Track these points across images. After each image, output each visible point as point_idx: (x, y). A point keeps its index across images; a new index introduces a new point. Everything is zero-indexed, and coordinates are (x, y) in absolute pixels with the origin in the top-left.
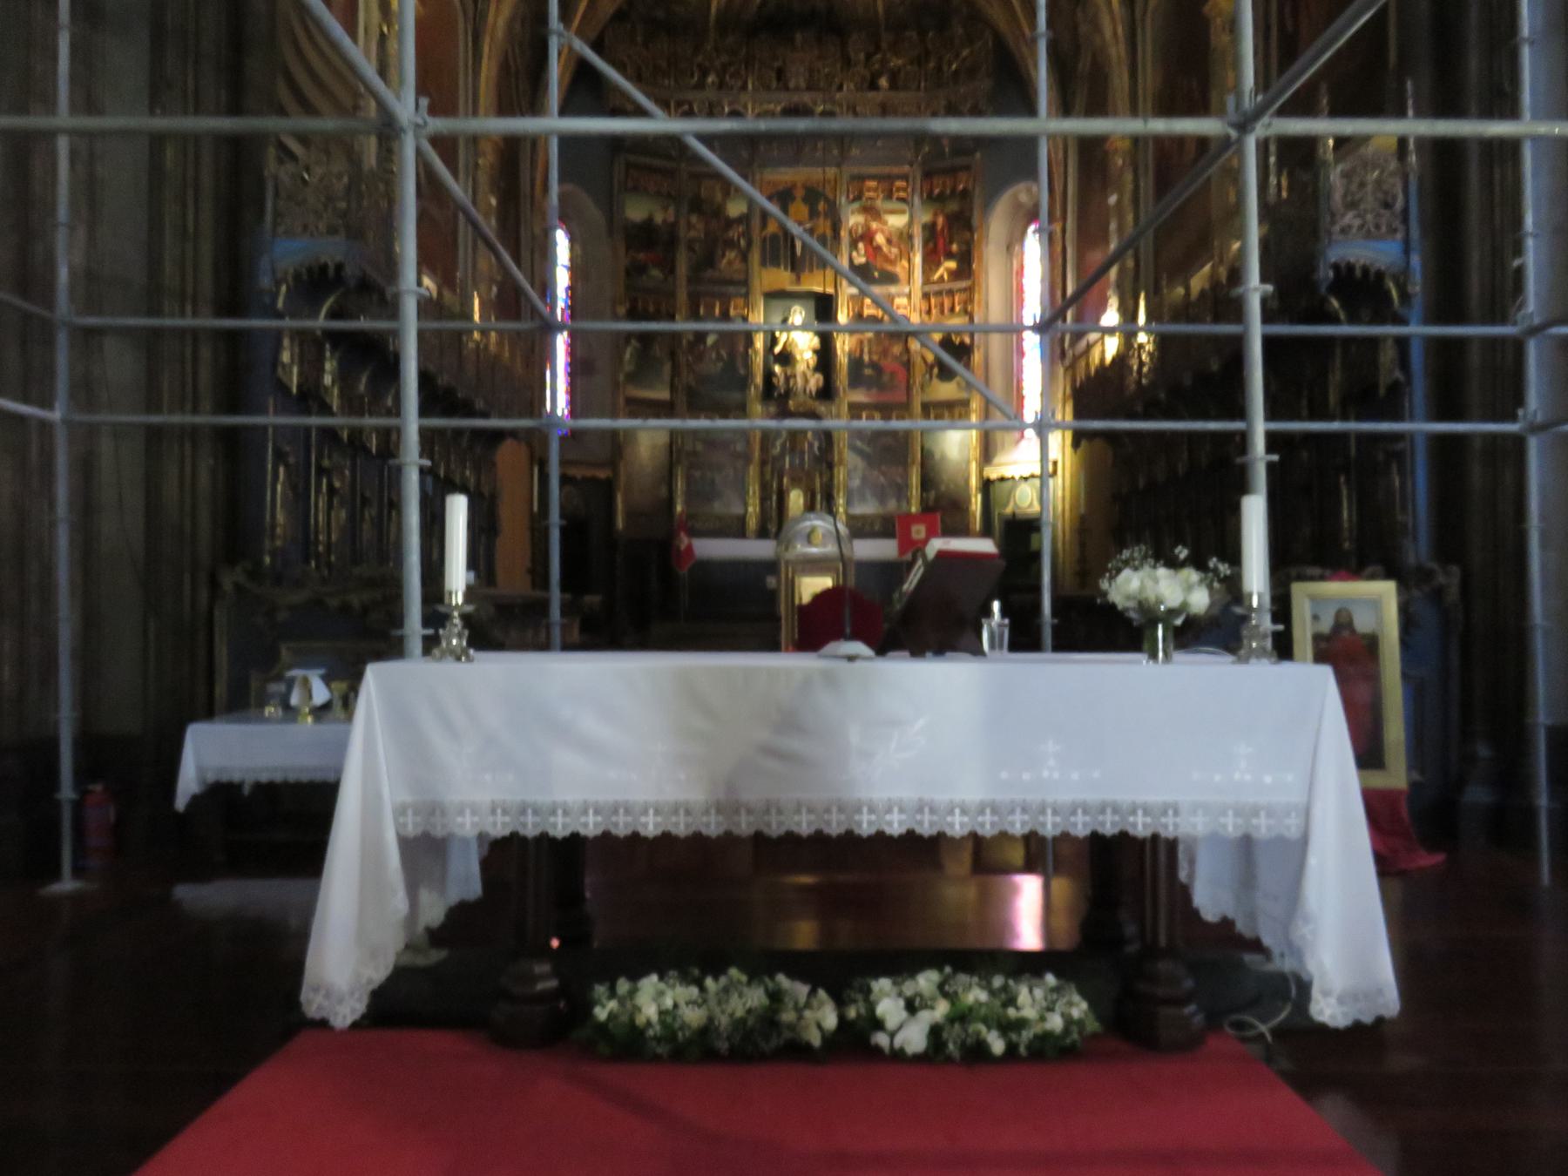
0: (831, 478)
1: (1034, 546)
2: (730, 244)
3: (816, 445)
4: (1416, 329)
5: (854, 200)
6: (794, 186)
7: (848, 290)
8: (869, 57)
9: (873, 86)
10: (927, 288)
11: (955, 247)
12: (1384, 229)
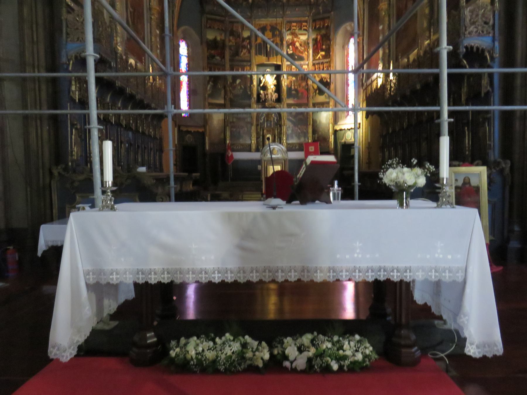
1: (352, 154)
2: (244, 47)
3: (276, 118)
4: (496, 70)
5: (288, 30)
6: (267, 25)
7: (286, 63)
10: (314, 62)
11: (324, 47)
12: (485, 32)
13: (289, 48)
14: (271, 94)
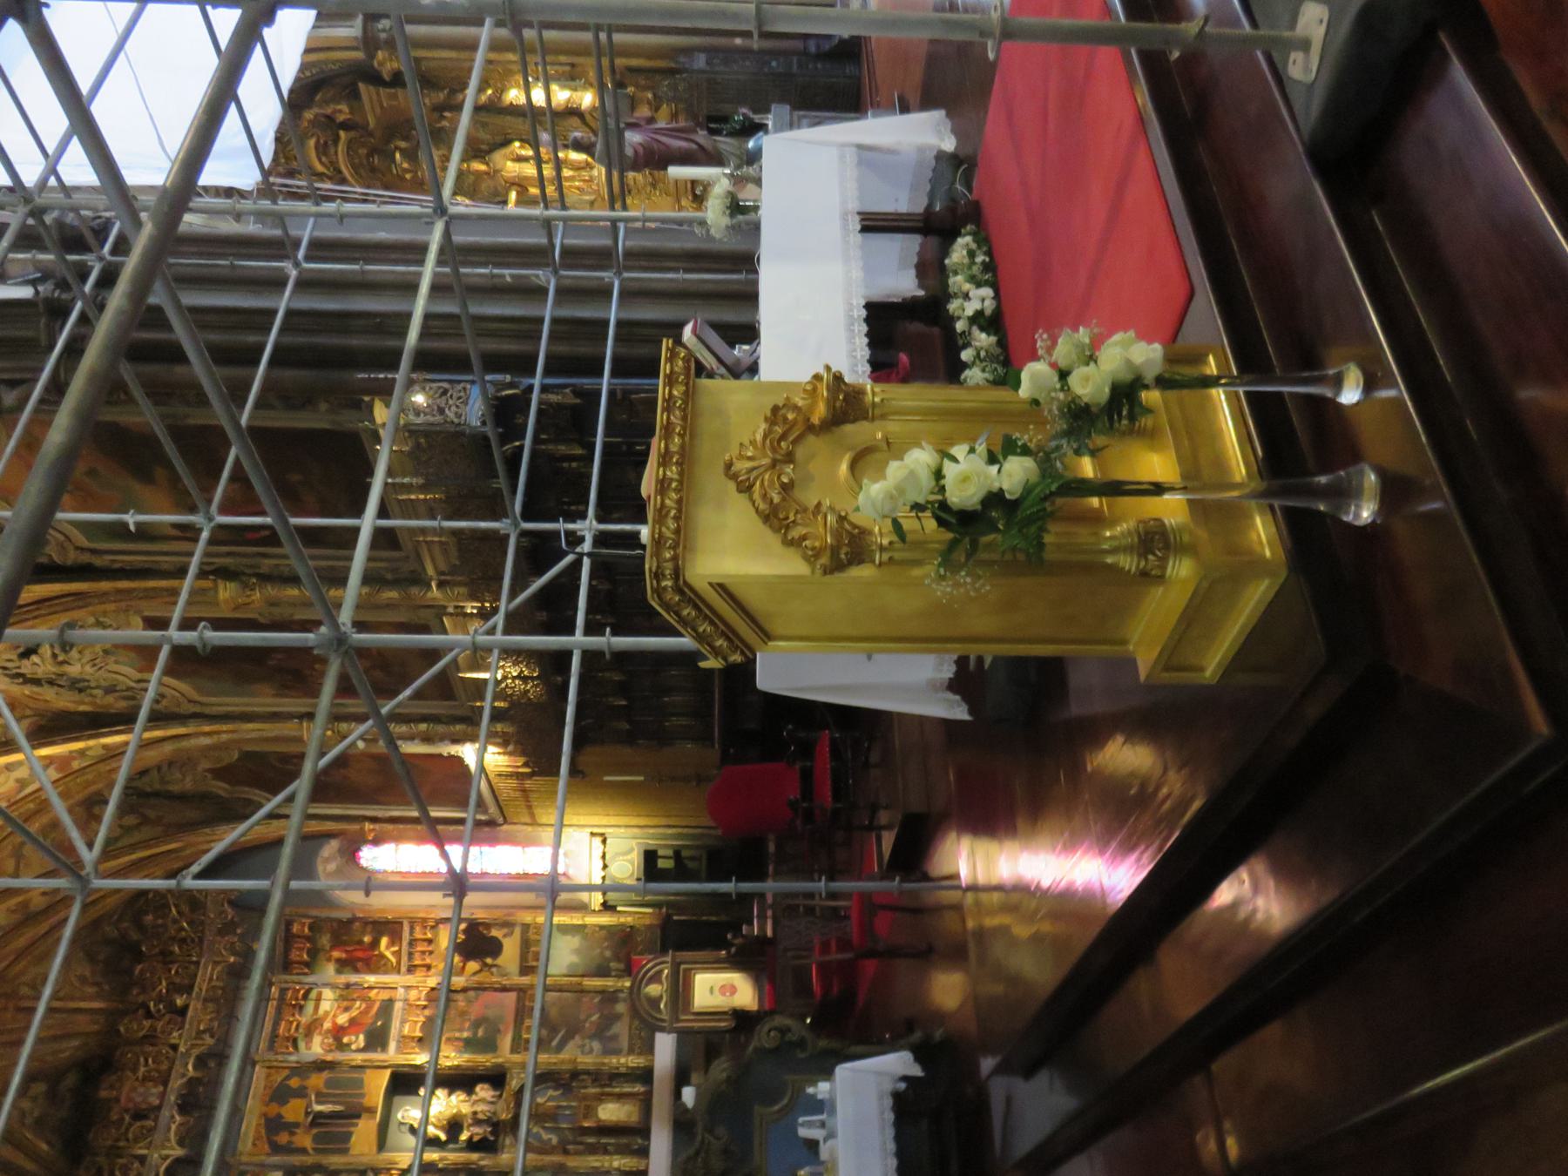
0: (587, 1072)
3: (551, 1092)
4: (537, 381)
5: (296, 1046)
7: (392, 1054)
8: (149, 1015)
9: (183, 1011)
10: (403, 969)
11: (367, 939)
13: (348, 1045)
14: (476, 1102)
